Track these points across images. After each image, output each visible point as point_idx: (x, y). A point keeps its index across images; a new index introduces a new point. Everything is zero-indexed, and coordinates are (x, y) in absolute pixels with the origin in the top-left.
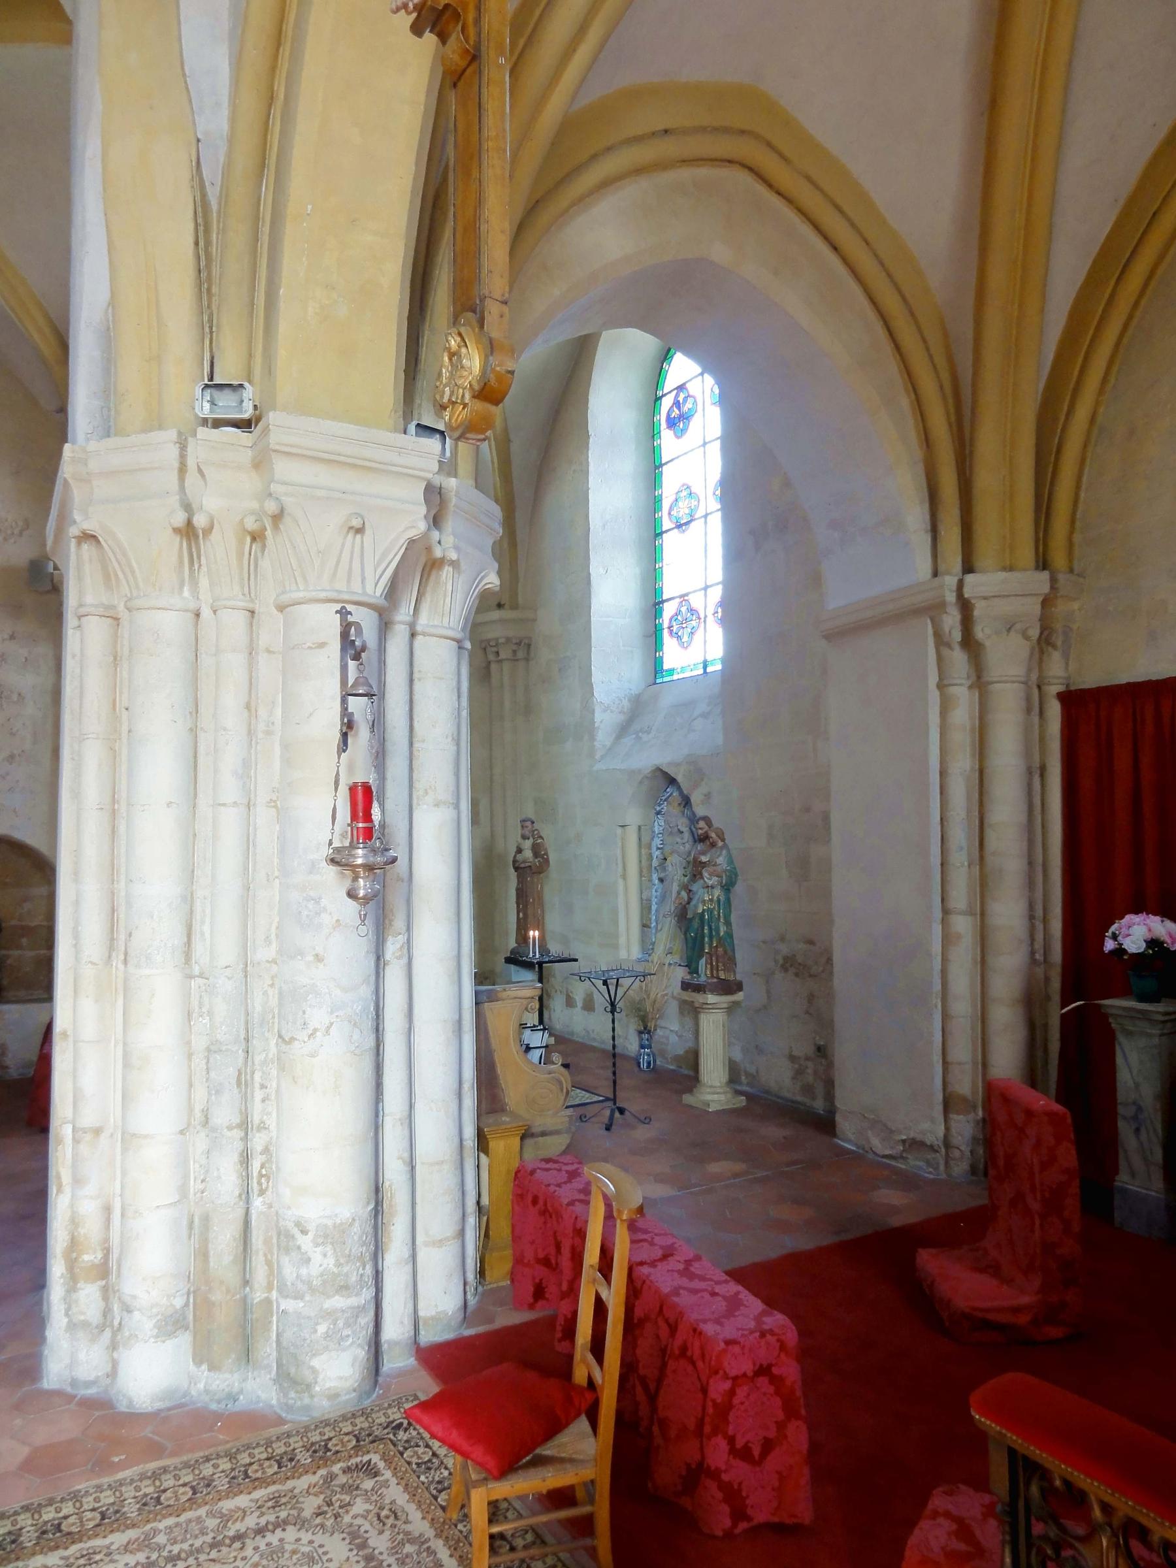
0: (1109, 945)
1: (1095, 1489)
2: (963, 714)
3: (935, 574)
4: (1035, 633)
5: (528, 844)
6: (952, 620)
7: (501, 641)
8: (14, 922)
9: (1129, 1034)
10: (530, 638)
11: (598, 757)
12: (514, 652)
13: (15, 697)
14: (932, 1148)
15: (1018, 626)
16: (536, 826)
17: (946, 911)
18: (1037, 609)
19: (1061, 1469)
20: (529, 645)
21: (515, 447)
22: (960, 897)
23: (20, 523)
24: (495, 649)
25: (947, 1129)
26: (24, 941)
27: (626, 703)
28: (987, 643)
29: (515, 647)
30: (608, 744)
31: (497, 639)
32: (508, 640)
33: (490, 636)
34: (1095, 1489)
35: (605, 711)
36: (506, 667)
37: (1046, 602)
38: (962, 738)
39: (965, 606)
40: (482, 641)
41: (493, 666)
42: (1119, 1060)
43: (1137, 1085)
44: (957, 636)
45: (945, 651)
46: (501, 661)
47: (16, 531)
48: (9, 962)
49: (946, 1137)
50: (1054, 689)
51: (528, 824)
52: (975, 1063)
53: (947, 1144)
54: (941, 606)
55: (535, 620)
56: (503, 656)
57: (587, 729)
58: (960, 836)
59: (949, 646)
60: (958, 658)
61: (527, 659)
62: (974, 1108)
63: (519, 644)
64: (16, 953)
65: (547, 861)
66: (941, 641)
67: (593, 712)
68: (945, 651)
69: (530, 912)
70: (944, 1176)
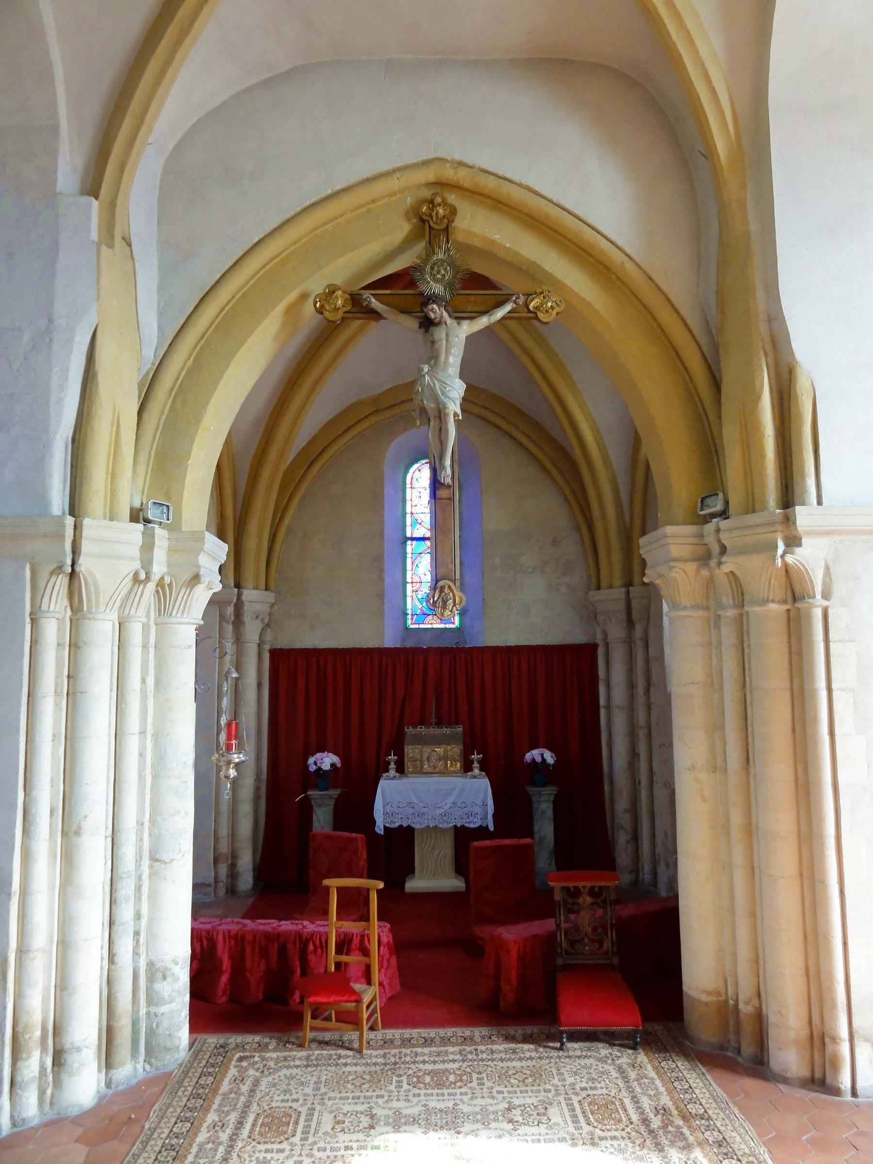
0: (313, 768)
1: (580, 884)
6: (230, 610)
9: (319, 806)
14: (209, 885)
15: (260, 617)
18: (268, 610)
19: (571, 885)
25: (216, 873)
28: (247, 624)
34: (580, 884)
37: (272, 605)
39: (239, 606)
42: (315, 818)
43: (322, 828)
45: (224, 624)
49: (215, 877)
50: (267, 647)
52: (228, 836)
53: (216, 880)
54: (228, 603)
59: (228, 622)
60: (230, 628)
62: (227, 859)
68: (224, 624)
70: (213, 899)
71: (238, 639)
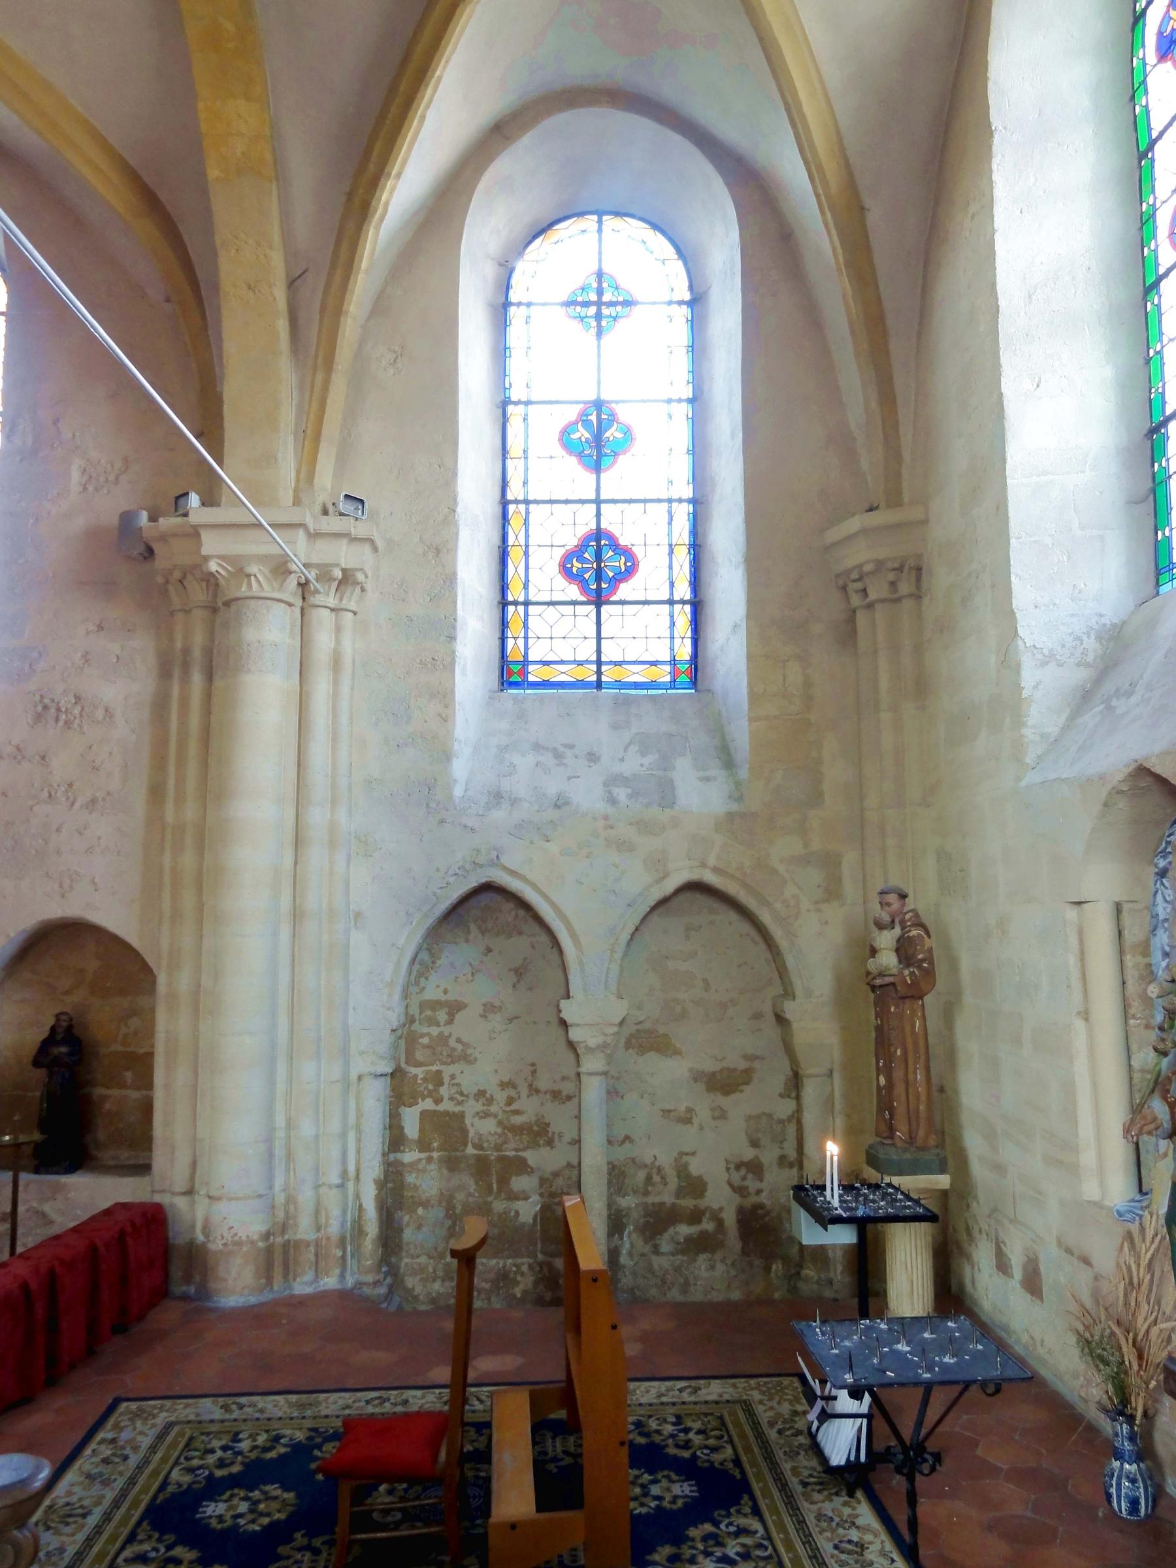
5: (886, 940)
7: (868, 568)
8: (117, 1047)
10: (919, 556)
11: (1030, 759)
12: (893, 584)
13: (100, 714)
16: (910, 903)
20: (919, 569)
21: (874, 218)
23: (118, 465)
24: (859, 585)
26: (129, 1075)
27: (1091, 644)
29: (891, 576)
30: (1053, 729)
31: (860, 566)
32: (880, 564)
33: (850, 562)
35: (1044, 664)
36: (880, 612)
40: (838, 576)
41: (862, 619)
46: (870, 606)
47: (112, 478)
48: (107, 1106)
51: (892, 898)
55: (925, 522)
56: (873, 595)
57: (1009, 705)
61: (917, 597)
63: (900, 569)
64: (115, 1092)
65: (930, 974)
67: (1017, 669)
69: (898, 1074)
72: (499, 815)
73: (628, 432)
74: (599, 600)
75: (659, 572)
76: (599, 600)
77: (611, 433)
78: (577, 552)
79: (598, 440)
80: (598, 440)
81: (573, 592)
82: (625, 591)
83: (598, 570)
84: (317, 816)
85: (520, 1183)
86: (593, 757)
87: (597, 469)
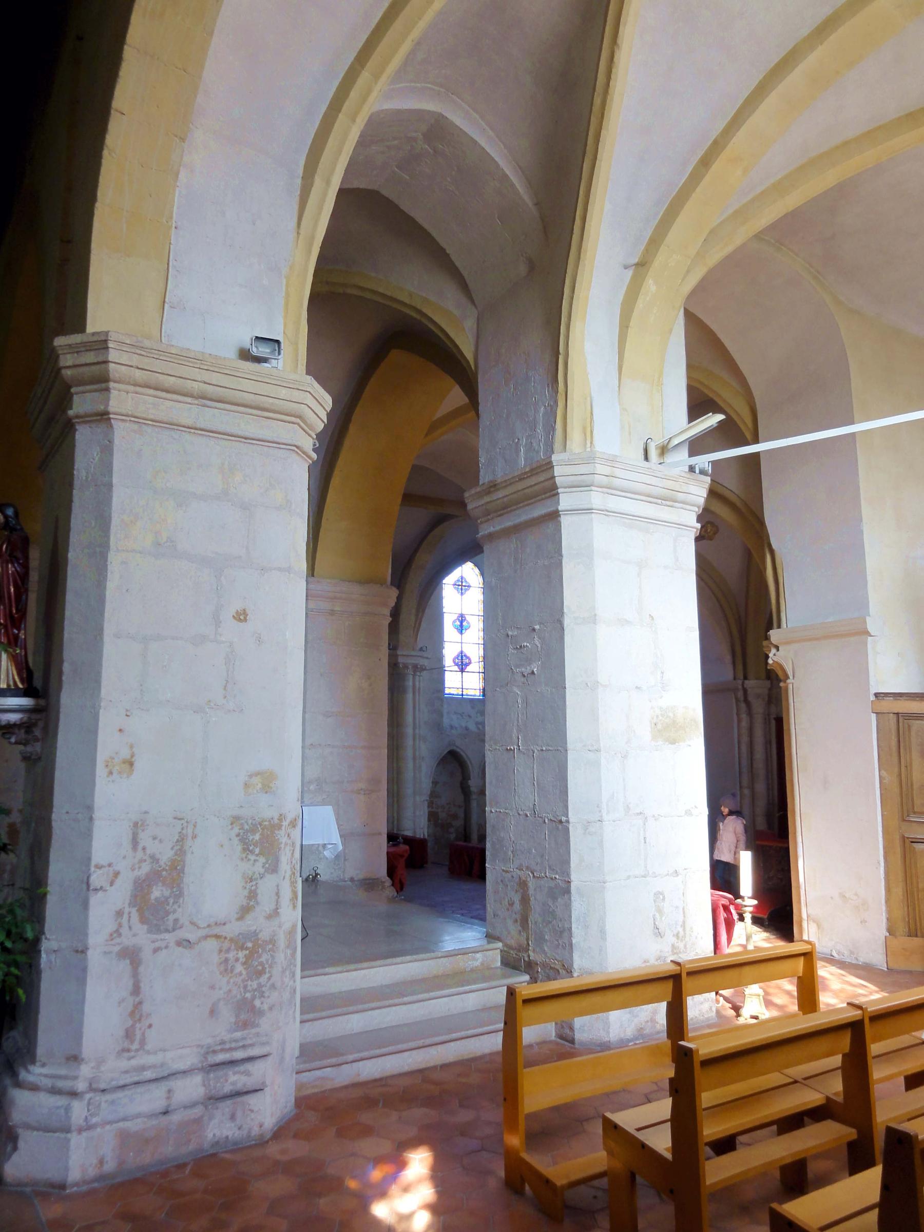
2: (744, 724)
3: (735, 679)
4: (767, 699)
6: (740, 694)
17: (741, 787)
22: (745, 782)
37: (770, 689)
38: (745, 732)
39: (745, 691)
44: (742, 699)
58: (745, 762)
66: (737, 700)
71: (750, 714)
72: (454, 732)
73: (468, 623)
74: (462, 671)
75: (476, 666)
76: (462, 671)
77: (464, 623)
78: (457, 657)
79: (461, 625)
80: (461, 625)
81: (456, 668)
82: (469, 669)
83: (462, 663)
84: (417, 731)
85: (452, 830)
86: (470, 716)
87: (461, 633)
